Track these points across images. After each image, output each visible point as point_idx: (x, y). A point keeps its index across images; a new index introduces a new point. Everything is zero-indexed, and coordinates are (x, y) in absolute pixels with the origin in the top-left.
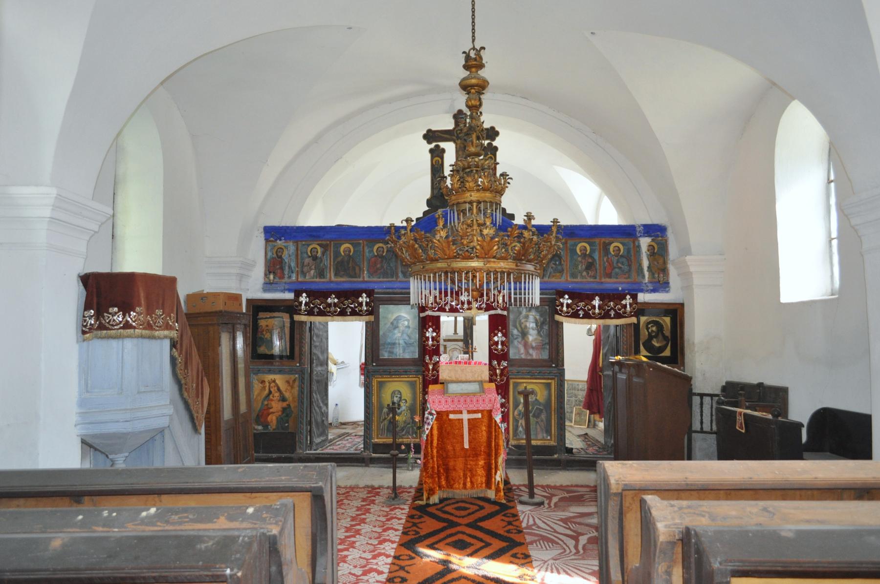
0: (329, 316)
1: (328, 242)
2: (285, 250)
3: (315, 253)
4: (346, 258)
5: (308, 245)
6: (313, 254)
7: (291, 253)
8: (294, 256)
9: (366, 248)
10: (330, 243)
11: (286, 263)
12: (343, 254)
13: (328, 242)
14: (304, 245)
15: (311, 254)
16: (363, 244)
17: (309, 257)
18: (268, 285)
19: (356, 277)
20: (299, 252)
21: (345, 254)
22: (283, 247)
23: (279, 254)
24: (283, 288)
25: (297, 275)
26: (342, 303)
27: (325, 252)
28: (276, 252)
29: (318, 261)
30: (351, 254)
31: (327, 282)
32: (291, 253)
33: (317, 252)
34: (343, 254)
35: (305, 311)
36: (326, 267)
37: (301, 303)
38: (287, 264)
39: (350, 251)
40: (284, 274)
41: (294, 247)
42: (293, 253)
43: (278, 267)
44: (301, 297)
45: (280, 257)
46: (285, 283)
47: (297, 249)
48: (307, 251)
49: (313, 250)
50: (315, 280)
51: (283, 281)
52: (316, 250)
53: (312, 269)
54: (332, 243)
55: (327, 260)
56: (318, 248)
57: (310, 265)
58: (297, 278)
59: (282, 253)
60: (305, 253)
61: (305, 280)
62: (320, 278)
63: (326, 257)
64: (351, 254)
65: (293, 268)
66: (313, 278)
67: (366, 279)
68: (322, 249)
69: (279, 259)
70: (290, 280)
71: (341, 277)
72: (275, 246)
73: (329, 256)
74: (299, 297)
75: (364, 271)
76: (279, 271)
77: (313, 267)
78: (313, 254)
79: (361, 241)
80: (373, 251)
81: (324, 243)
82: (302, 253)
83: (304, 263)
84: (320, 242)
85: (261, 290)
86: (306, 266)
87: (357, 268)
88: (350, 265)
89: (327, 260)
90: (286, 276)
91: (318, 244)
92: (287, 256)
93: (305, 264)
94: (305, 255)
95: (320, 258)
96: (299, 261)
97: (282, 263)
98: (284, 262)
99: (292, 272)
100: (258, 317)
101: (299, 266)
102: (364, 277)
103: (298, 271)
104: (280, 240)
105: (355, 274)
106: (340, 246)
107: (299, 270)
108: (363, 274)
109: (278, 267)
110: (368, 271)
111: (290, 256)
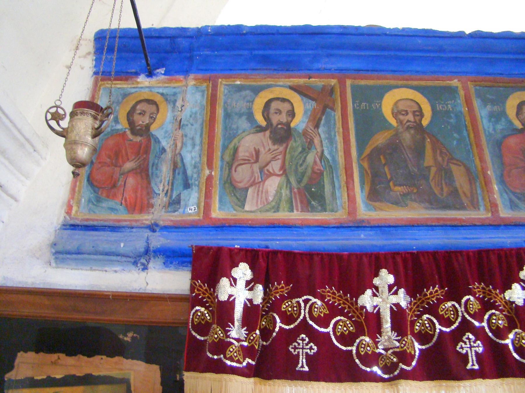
0: (373, 378)
1: (333, 82)
2: (162, 106)
3: (284, 118)
4: (407, 137)
5: (257, 90)
6: (275, 119)
7: (185, 115)
8: (197, 126)
9: (476, 103)
10: (342, 83)
11: (163, 150)
12: (393, 122)
13: (333, 82)
14: (240, 89)
15: (267, 118)
16: (466, 89)
17: (261, 129)
18: (79, 235)
19: (462, 207)
20: (220, 112)
21: (400, 122)
22: (158, 99)
23: (141, 121)
24: (141, 246)
25: (208, 195)
26: (433, 310)
27: (323, 112)
28: (130, 115)
29: (296, 144)
30: (425, 122)
31: (340, 227)
32: (185, 115)
33: (292, 114)
34: (393, 122)
35: (248, 352)
36: (332, 169)
37: (230, 304)
38: (169, 155)
39: (420, 113)
40: (150, 193)
41: (198, 96)
42: (193, 115)
43: (129, 165)
44: (224, 282)
45: (146, 131)
46: (153, 228)
47: (213, 101)
48: (250, 109)
49: (274, 105)
50: (283, 215)
51: (147, 218)
52: (286, 107)
53: (271, 174)
54: (349, 82)
55: (331, 140)
56: (296, 99)
57: (264, 157)
58: (207, 208)
59: (153, 119)
60: (240, 115)
61: (241, 215)
62: (307, 207)
63: (329, 132)
64: (425, 122)
65: (189, 172)
66: (277, 209)
67: (505, 213)
68: (312, 105)
69: (138, 139)
70: (175, 217)
71: (397, 203)
72: (125, 95)
73: (339, 124)
74: (213, 283)
75: (487, 183)
76: (131, 181)
77: (275, 166)
78: (275, 119)
79: (455, 83)
80: (503, 114)
81: (317, 82)
82: (227, 116)
83: (236, 150)
84: (302, 81)
85: (48, 254)
86: (246, 161)
87: (458, 173)
88: (428, 160)
89: (331, 140)
90: (160, 200)
91: (291, 88)
92: (169, 127)
93: (242, 154)
94: (243, 124)
95: (305, 133)
96: (219, 142)
97: (147, 151)
98: (154, 148)
99: (187, 185)
100: (7, 376)
101: (217, 163)
102: (493, 207)
103: (210, 178)
104: (150, 74)
105: (455, 193)
106: (381, 97)
107: (216, 174)
108: (490, 191)
109: (129, 165)
110: (502, 181)
111: (180, 125)
